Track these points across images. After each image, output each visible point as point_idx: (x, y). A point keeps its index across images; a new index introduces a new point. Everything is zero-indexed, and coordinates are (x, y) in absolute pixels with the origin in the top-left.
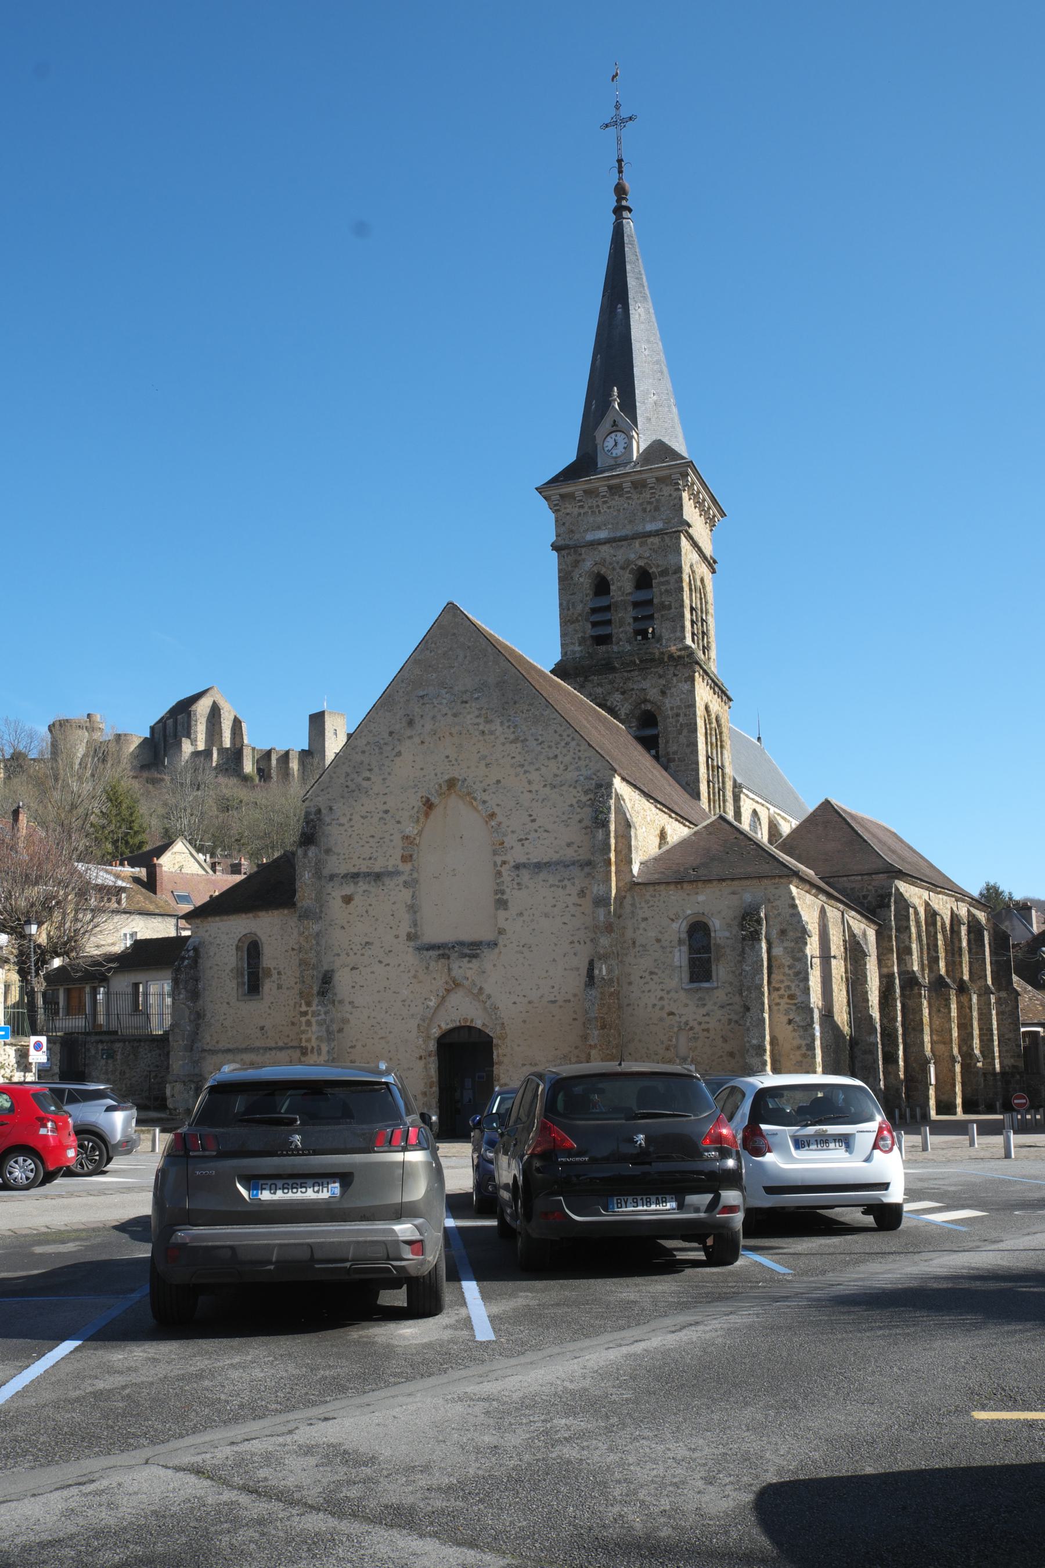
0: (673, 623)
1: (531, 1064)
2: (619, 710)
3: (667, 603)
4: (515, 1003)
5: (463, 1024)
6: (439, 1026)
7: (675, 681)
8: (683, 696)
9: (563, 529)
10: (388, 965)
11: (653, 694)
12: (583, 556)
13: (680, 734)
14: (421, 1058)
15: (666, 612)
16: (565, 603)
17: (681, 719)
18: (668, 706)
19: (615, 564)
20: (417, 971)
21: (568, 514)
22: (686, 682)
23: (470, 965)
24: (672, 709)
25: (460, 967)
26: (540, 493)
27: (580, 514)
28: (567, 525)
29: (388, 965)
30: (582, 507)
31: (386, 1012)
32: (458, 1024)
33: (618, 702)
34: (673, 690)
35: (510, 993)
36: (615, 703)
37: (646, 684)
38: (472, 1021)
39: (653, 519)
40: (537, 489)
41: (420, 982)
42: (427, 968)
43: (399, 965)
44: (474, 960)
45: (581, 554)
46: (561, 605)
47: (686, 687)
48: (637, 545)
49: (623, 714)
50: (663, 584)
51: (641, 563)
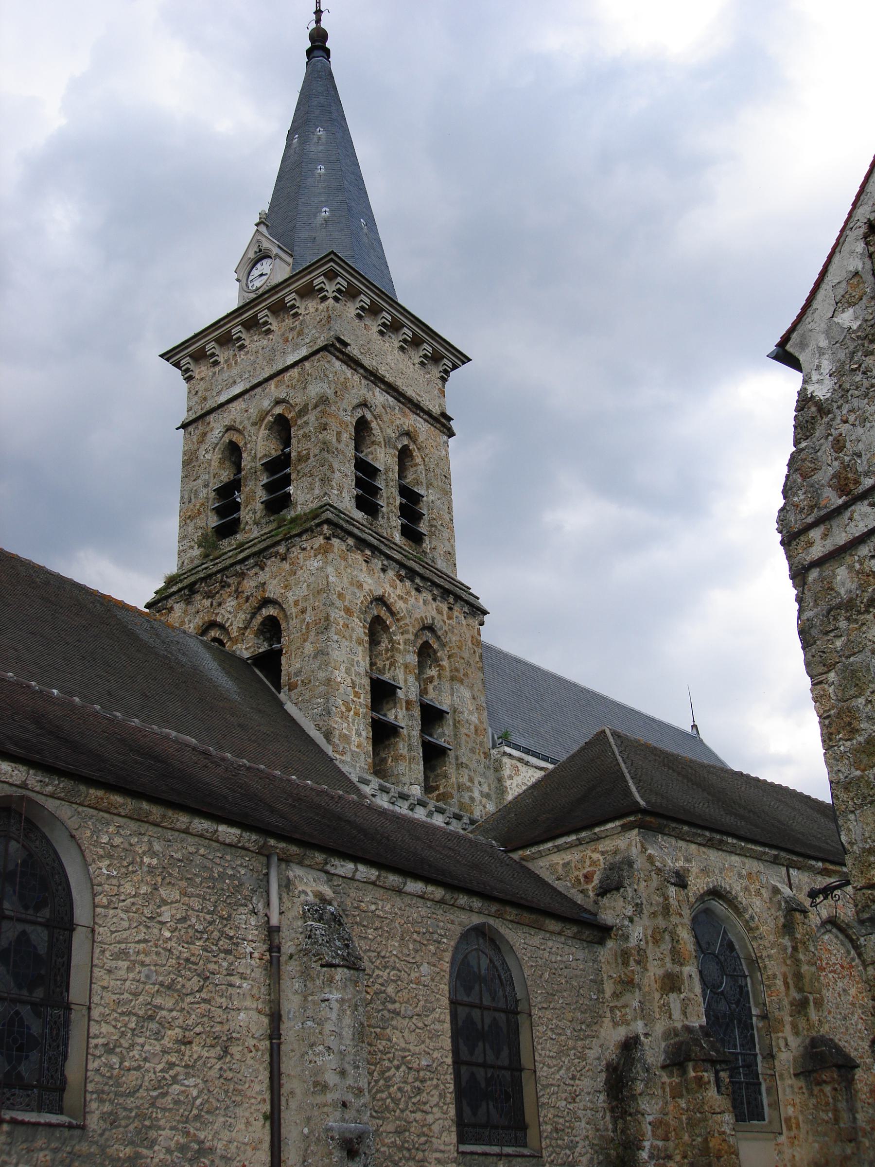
0: (310, 479)
2: (231, 625)
3: (305, 452)
7: (302, 560)
8: (312, 579)
9: (196, 399)
11: (274, 590)
12: (212, 424)
13: (305, 641)
15: (304, 465)
16: (186, 496)
17: (309, 617)
18: (291, 599)
19: (246, 422)
21: (202, 379)
22: (315, 556)
24: (296, 603)
26: (168, 360)
27: (215, 373)
28: (200, 393)
30: (216, 363)
33: (230, 613)
34: (300, 572)
36: (227, 615)
37: (263, 576)
39: (296, 347)
40: (162, 356)
45: (209, 423)
46: (182, 497)
47: (316, 564)
48: (273, 386)
49: (235, 629)
50: (301, 427)
51: (278, 410)
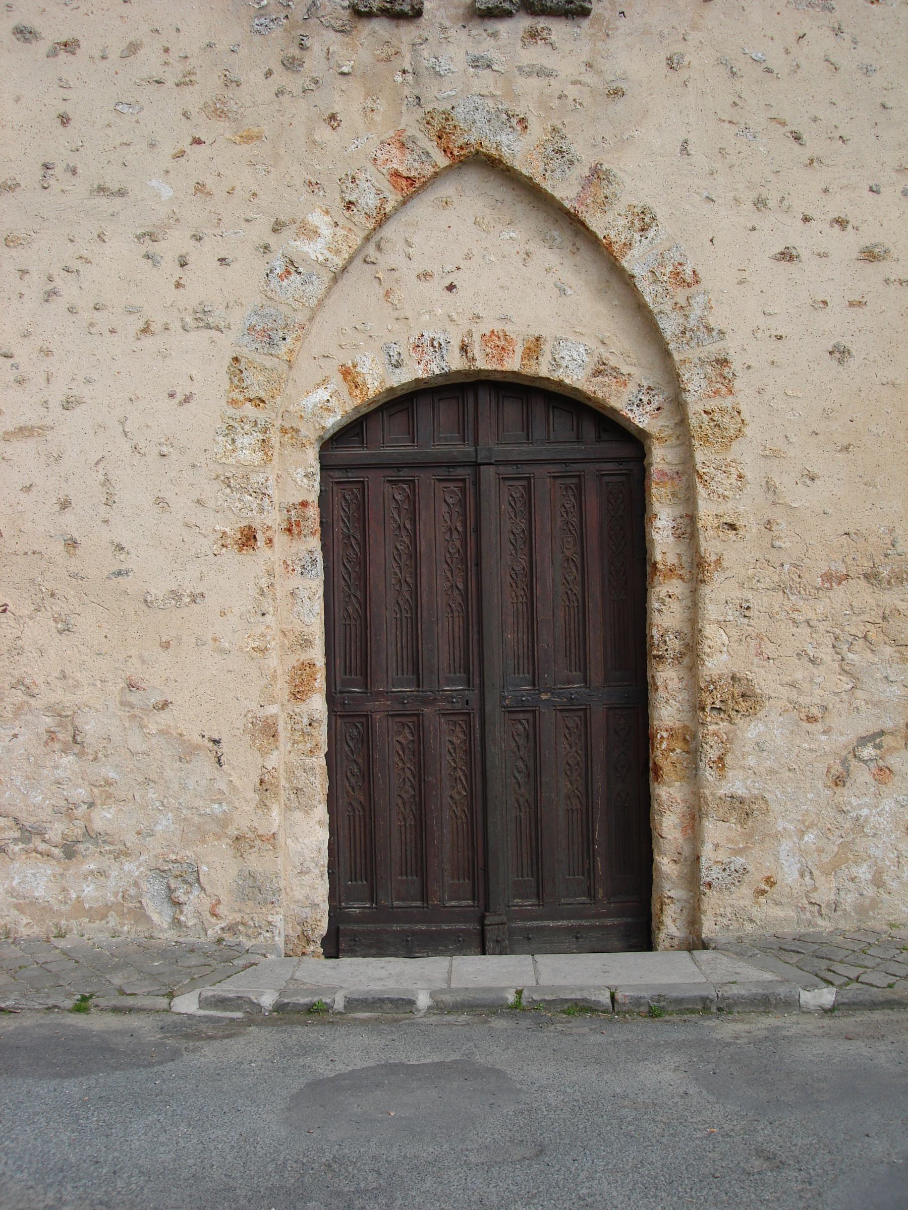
1: (871, 577)
4: (787, 256)
5: (482, 364)
6: (347, 373)
10: (69, 46)
14: (248, 538)
20: (231, 82)
23: (535, 55)
25: (477, 63)
29: (69, 46)
31: (51, 295)
32: (456, 363)
35: (760, 203)
38: (534, 348)
41: (248, 139)
42: (291, 64)
43: (133, 48)
44: (559, 29)
